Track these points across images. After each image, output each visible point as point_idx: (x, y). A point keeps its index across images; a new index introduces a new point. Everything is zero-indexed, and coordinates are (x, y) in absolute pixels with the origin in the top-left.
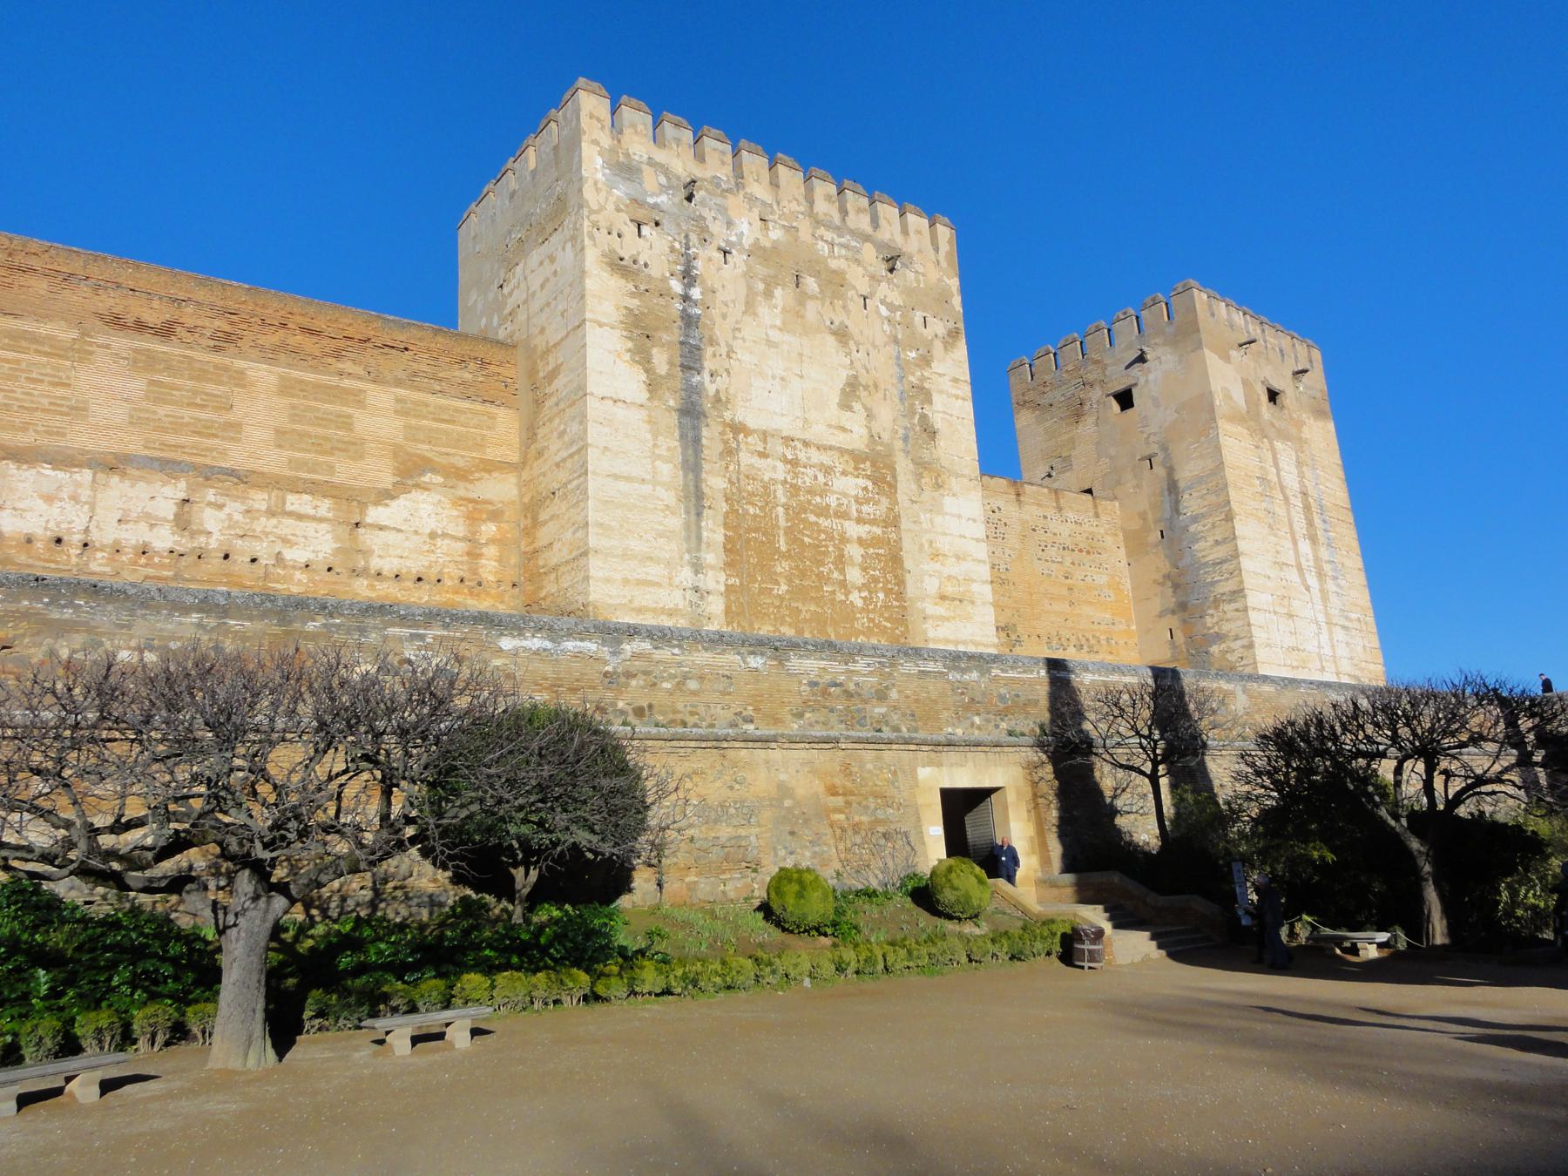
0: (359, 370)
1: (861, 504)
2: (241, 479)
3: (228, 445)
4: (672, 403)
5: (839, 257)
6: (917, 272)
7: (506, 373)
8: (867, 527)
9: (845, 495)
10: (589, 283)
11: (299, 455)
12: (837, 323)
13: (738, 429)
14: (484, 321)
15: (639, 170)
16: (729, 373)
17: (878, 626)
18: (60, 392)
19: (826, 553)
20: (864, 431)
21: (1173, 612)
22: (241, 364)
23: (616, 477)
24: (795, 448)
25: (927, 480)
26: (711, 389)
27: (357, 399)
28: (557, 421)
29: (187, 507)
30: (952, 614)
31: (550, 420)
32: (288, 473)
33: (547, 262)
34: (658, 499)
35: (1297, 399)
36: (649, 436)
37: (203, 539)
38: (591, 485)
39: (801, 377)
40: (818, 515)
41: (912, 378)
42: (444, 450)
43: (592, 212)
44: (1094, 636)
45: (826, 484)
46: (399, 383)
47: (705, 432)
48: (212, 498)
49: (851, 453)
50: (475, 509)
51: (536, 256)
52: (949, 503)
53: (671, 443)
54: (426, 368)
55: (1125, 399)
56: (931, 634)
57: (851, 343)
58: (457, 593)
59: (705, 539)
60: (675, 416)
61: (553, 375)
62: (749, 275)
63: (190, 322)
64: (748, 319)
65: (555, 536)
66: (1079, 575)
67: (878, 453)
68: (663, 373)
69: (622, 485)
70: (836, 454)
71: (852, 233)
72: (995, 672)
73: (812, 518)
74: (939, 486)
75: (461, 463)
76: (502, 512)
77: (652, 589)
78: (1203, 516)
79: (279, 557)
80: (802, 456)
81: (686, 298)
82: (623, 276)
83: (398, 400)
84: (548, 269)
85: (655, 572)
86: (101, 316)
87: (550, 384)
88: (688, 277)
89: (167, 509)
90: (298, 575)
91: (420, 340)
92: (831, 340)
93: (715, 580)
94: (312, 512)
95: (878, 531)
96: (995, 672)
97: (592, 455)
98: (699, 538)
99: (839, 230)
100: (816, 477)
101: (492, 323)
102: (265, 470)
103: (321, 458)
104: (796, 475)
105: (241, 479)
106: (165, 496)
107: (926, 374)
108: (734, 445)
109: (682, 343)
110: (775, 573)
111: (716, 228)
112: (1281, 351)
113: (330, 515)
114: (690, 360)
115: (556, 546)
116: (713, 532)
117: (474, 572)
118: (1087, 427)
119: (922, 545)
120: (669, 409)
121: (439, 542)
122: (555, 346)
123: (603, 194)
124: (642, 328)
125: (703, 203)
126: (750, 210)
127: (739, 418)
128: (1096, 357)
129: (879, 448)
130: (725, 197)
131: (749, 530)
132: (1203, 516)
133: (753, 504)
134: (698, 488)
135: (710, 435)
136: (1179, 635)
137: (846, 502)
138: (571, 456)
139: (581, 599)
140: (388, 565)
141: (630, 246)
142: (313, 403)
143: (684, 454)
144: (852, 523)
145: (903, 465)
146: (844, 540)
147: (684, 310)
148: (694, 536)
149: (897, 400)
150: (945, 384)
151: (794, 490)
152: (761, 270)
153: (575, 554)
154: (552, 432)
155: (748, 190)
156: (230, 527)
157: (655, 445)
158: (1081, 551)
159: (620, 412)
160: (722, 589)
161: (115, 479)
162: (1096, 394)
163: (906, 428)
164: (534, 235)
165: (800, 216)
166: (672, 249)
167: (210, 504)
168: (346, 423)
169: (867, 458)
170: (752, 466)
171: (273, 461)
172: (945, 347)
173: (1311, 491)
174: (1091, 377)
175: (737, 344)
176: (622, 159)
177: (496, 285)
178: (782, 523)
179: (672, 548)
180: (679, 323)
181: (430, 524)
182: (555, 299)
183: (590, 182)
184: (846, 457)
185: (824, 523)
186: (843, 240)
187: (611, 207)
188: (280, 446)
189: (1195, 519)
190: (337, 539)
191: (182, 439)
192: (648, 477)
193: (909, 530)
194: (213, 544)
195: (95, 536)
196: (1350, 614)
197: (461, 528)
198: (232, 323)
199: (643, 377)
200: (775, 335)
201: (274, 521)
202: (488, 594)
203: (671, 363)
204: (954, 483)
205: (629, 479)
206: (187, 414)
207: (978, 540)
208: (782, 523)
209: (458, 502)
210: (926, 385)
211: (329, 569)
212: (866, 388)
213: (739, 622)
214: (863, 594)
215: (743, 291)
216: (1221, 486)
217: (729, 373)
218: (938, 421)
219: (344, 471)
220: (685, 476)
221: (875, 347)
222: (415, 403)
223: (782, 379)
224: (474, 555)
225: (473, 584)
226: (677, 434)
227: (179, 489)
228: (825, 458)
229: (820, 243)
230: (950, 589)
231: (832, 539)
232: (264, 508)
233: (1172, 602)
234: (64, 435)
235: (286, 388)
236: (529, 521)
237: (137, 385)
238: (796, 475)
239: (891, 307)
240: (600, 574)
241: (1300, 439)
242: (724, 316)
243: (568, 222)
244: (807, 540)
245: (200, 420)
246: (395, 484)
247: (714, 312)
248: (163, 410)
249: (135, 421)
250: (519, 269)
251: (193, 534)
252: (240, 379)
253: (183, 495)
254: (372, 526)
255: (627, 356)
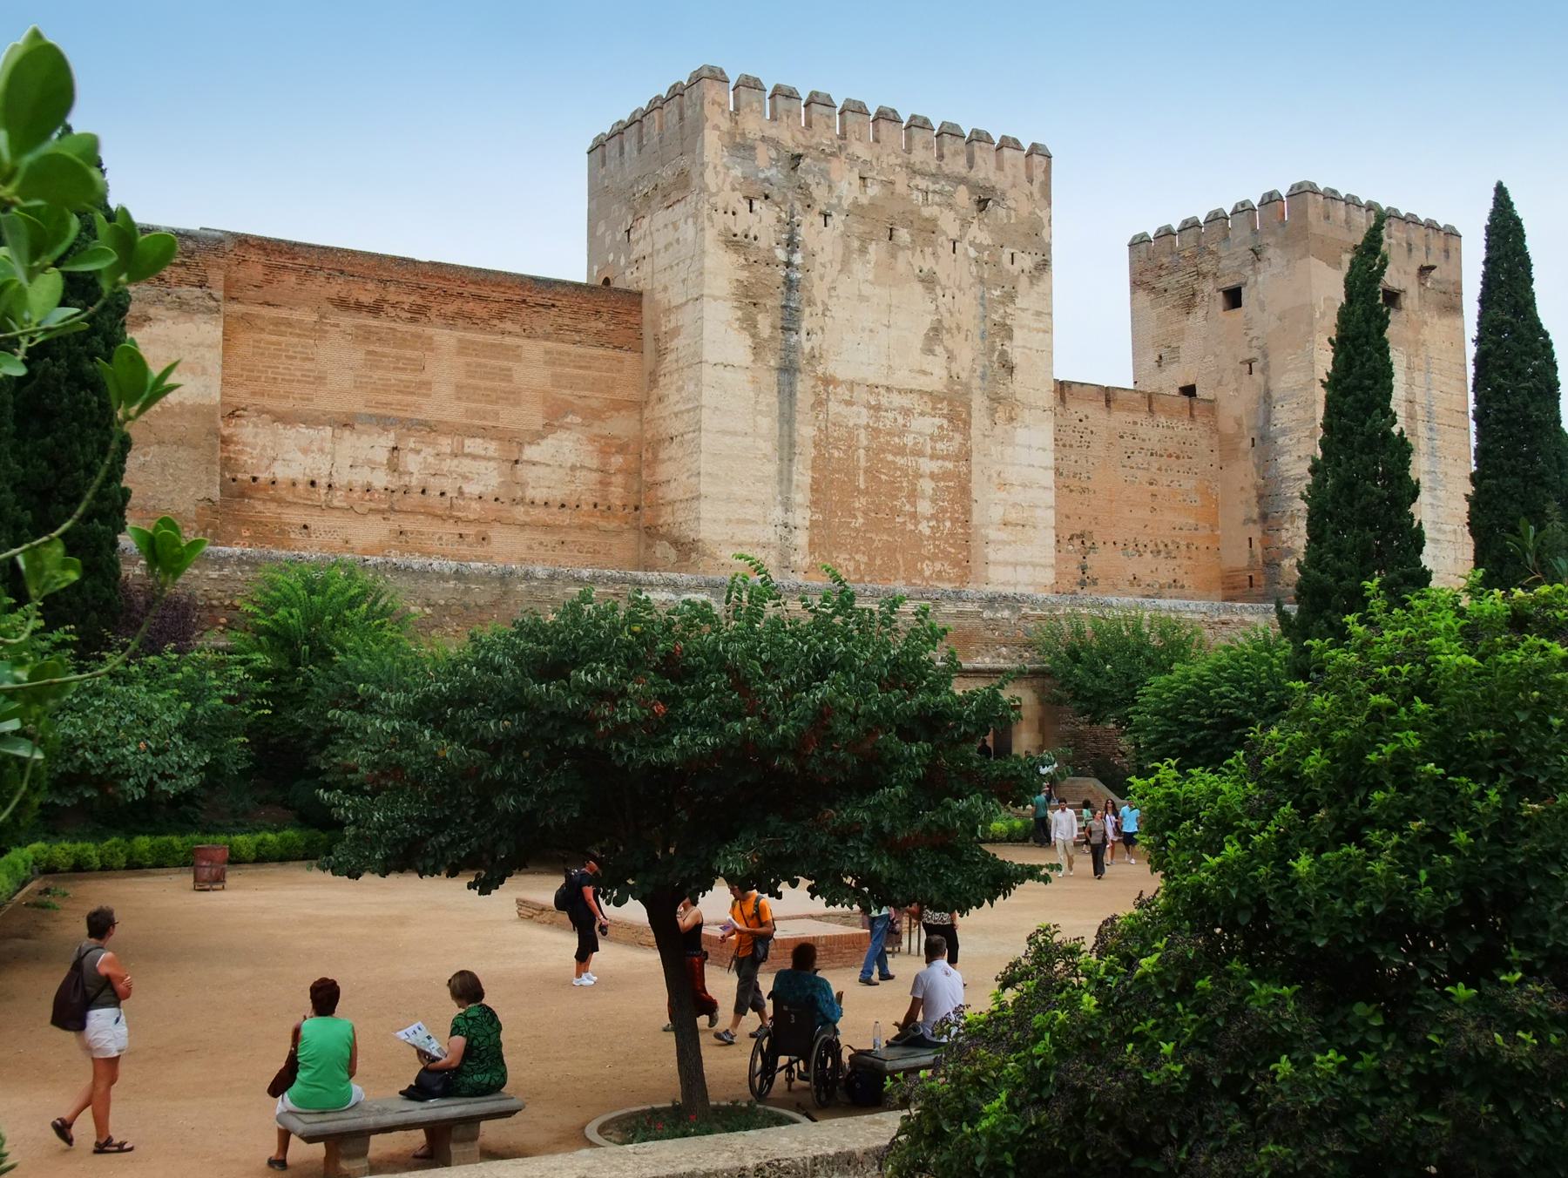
0: (517, 329)
1: (936, 442)
2: (431, 428)
3: (421, 400)
4: (772, 363)
5: (932, 205)
6: (1009, 208)
7: (632, 320)
8: (940, 462)
9: (920, 434)
10: (708, 263)
11: (473, 405)
12: (925, 270)
13: (828, 381)
14: (611, 257)
15: (753, 148)
16: (823, 330)
17: (942, 552)
18: (308, 365)
19: (900, 489)
20: (944, 373)
21: (1254, 522)
22: (429, 331)
23: (724, 432)
24: (878, 394)
25: (1001, 415)
26: (807, 347)
27: (515, 354)
28: (676, 376)
29: (396, 453)
30: (1013, 538)
31: (671, 373)
32: (465, 421)
33: (671, 227)
34: (757, 449)
35: (1421, 297)
36: (752, 394)
37: (407, 478)
38: (704, 441)
39: (889, 327)
40: (895, 454)
41: (995, 317)
42: (582, 393)
43: (712, 195)
44: (1173, 542)
45: (905, 426)
46: (547, 337)
47: (799, 387)
48: (412, 445)
49: (931, 394)
50: (606, 444)
51: (661, 217)
52: (1021, 435)
53: (770, 399)
54: (567, 321)
55: (1233, 298)
56: (992, 556)
57: (939, 291)
58: (592, 515)
59: (794, 482)
60: (775, 374)
61: (675, 332)
62: (846, 235)
63: (392, 298)
64: (843, 277)
65: (672, 470)
66: (1164, 479)
67: (956, 392)
68: (766, 336)
69: (728, 440)
70: (915, 396)
71: (947, 177)
72: (1024, 610)
73: (890, 457)
74: (1012, 419)
75: (595, 403)
76: (628, 445)
77: (749, 527)
78: (1291, 430)
79: (461, 492)
80: (884, 401)
81: (788, 264)
82: (736, 251)
83: (547, 352)
84: (670, 235)
85: (752, 512)
86: (330, 300)
87: (671, 340)
88: (792, 244)
89: (382, 456)
90: (475, 505)
91: (565, 295)
92: (919, 288)
93: (802, 517)
94: (483, 453)
95: (949, 465)
96: (1024, 610)
97: (705, 414)
98: (790, 480)
99: (934, 177)
100: (896, 419)
101: (619, 261)
102: (448, 419)
103: (489, 407)
104: (878, 419)
105: (431, 428)
106: (377, 445)
107: (1008, 310)
108: (824, 397)
109: (784, 307)
110: (854, 509)
111: (819, 193)
112: (1409, 245)
113: (496, 455)
114: (789, 321)
115: (673, 485)
116: (802, 475)
117: (605, 498)
118: (1197, 319)
119: (990, 477)
120: (770, 368)
121: (578, 473)
122: (677, 307)
123: (722, 176)
124: (751, 297)
125: (807, 172)
126: (851, 170)
127: (830, 371)
128: (1213, 247)
129: (957, 387)
130: (829, 161)
131: (835, 471)
132: (1291, 430)
133: (839, 449)
134: (790, 436)
135: (804, 387)
136: (1258, 549)
137: (922, 441)
138: (688, 411)
139: (693, 535)
140: (539, 494)
141: (744, 222)
142: (483, 360)
143: (780, 409)
144: (926, 460)
145: (979, 402)
146: (919, 476)
147: (787, 275)
148: (785, 479)
149: (978, 340)
150: (1028, 319)
151: (875, 432)
152: (858, 228)
153: (688, 495)
154: (671, 383)
155: (850, 151)
156: (425, 468)
157: (757, 402)
158: (1170, 456)
159: (728, 375)
160: (807, 523)
161: (347, 433)
162: (1208, 287)
163: (984, 366)
164: (659, 198)
165: (898, 169)
166: (779, 220)
167: (411, 450)
168: (507, 375)
169: (942, 400)
170: (838, 414)
171: (453, 412)
172: (1031, 282)
173: (1421, 398)
174: (1205, 268)
175: (831, 303)
176: (738, 139)
177: (623, 228)
178: (863, 463)
179: (770, 490)
180: (783, 289)
181: (572, 459)
182: (678, 264)
183: (711, 166)
184: (926, 398)
185: (900, 461)
186: (937, 187)
187: (727, 187)
188: (459, 399)
189: (1284, 432)
190: (501, 474)
191: (390, 398)
192: (750, 431)
193: (979, 463)
194: (414, 482)
195: (336, 480)
196: (1444, 527)
197: (595, 461)
198: (422, 297)
199: (749, 341)
200: (867, 290)
201: (456, 462)
202: (615, 516)
203: (774, 327)
204: (1026, 416)
205: (734, 434)
206: (393, 377)
207: (1046, 468)
208: (863, 463)
209: (592, 440)
210: (1008, 322)
211: (496, 499)
212: (949, 331)
213: (820, 555)
214: (931, 524)
215: (840, 251)
216: (1309, 402)
217: (823, 330)
218: (1016, 356)
219: (509, 417)
220: (781, 428)
221: (960, 289)
222: (560, 353)
223: (871, 331)
224: (604, 484)
225: (604, 508)
226: (776, 389)
227: (389, 440)
228: (905, 401)
229: (915, 192)
230: (1013, 516)
231: (907, 475)
232: (449, 451)
233: (1255, 513)
234: (312, 400)
235: (463, 348)
236: (650, 455)
237: (359, 356)
238: (878, 419)
239: (980, 248)
240: (709, 516)
241: (1417, 342)
242: (822, 278)
243: (691, 198)
244: (883, 477)
245: (402, 381)
246: (544, 426)
247: (814, 275)
248: (377, 375)
249: (358, 386)
250: (645, 222)
251: (401, 474)
252: (428, 344)
253: (392, 444)
254: (527, 462)
255: (736, 325)
